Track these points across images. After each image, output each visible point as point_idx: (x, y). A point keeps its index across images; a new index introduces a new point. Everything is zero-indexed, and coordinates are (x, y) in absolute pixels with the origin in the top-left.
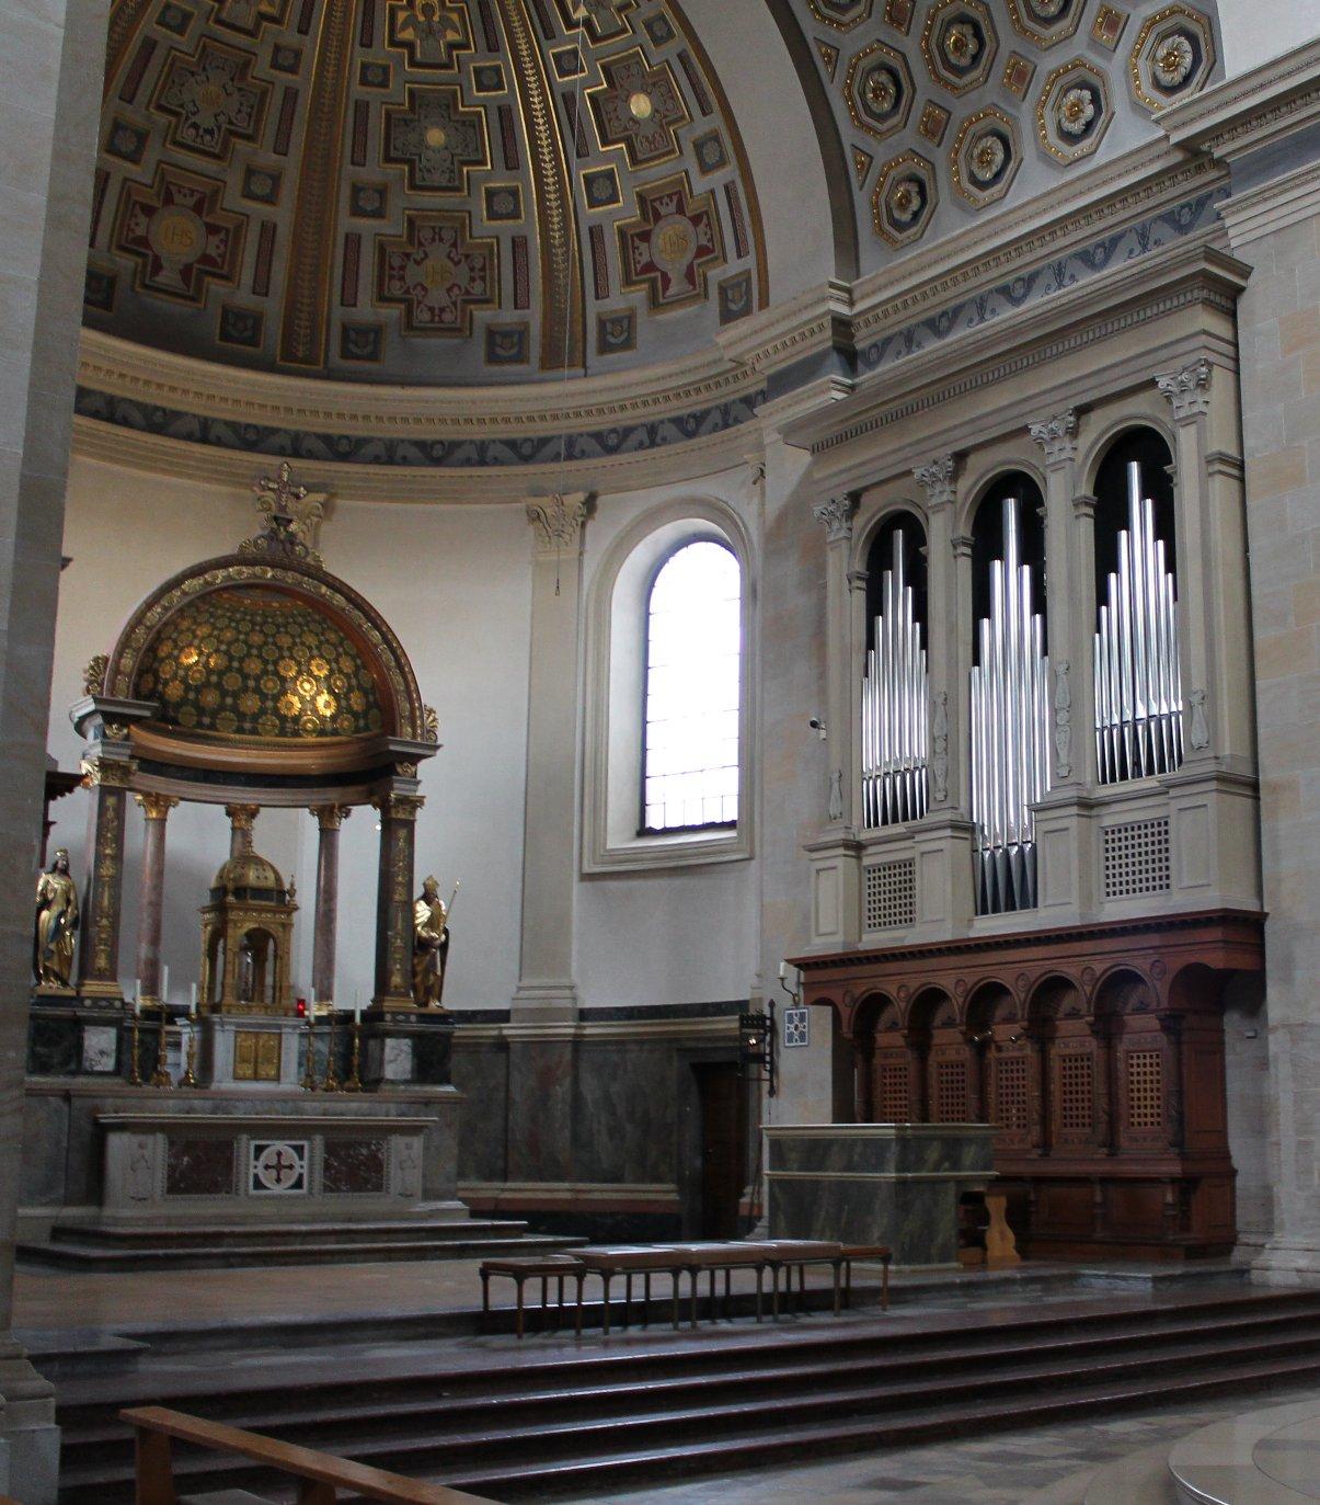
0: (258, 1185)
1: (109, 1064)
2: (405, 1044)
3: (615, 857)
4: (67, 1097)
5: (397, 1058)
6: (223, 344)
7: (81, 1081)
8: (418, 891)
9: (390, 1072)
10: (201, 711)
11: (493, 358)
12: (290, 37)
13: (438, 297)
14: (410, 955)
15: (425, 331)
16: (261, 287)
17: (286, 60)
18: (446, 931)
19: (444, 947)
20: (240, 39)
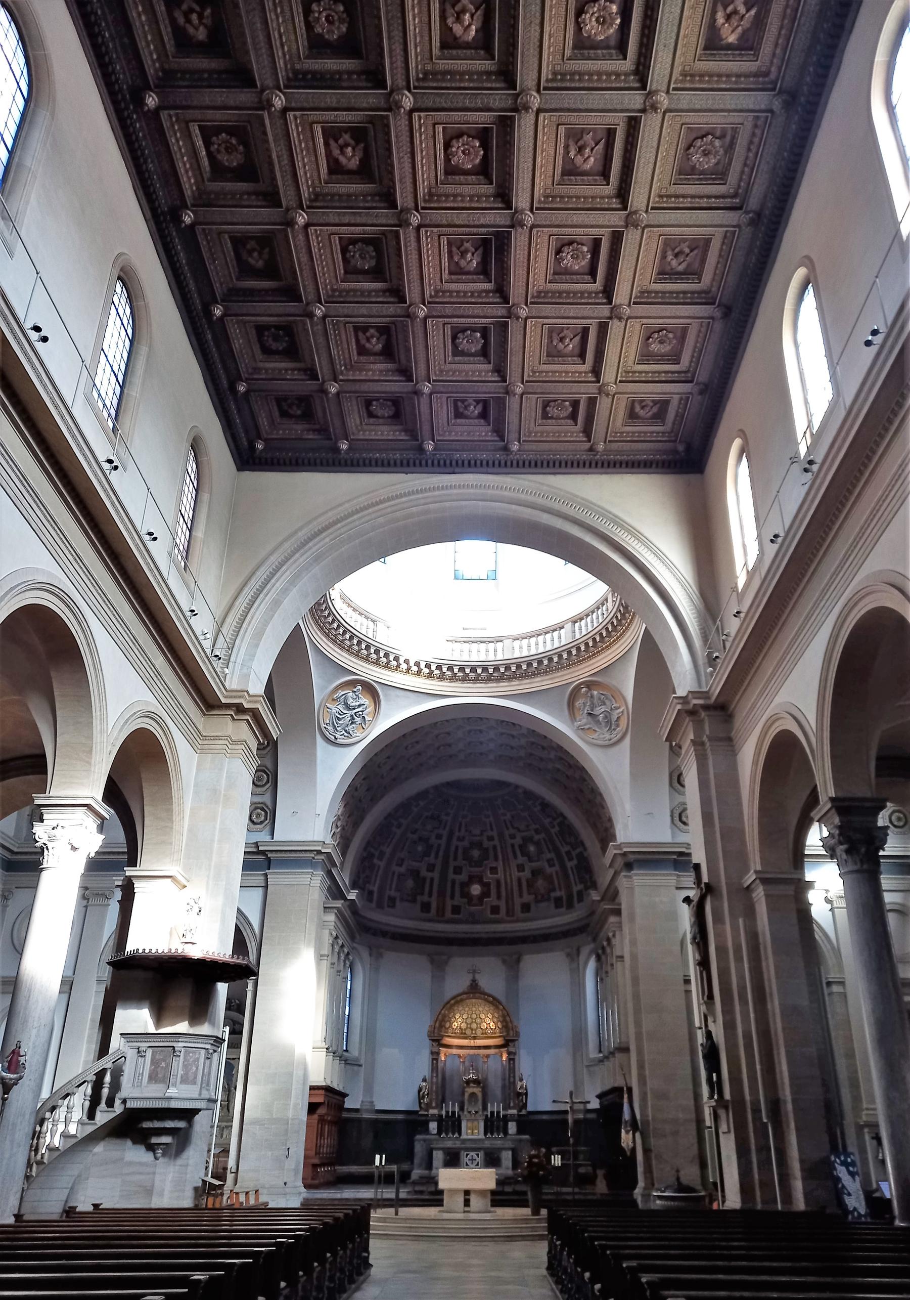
0: (467, 1165)
1: (435, 1132)
2: (514, 1123)
3: (593, 1060)
4: (425, 1140)
5: (512, 1127)
6: (493, 916)
7: (428, 1137)
8: (517, 1079)
9: (510, 1132)
10: (472, 1030)
11: (557, 907)
12: (490, 833)
13: (542, 891)
14: (521, 1097)
15: (541, 901)
16: (499, 897)
17: (491, 839)
18: (526, 1089)
19: (526, 1094)
20: (478, 838)
